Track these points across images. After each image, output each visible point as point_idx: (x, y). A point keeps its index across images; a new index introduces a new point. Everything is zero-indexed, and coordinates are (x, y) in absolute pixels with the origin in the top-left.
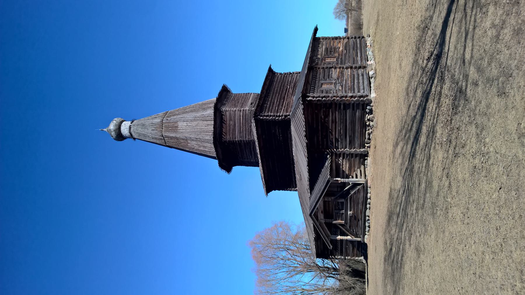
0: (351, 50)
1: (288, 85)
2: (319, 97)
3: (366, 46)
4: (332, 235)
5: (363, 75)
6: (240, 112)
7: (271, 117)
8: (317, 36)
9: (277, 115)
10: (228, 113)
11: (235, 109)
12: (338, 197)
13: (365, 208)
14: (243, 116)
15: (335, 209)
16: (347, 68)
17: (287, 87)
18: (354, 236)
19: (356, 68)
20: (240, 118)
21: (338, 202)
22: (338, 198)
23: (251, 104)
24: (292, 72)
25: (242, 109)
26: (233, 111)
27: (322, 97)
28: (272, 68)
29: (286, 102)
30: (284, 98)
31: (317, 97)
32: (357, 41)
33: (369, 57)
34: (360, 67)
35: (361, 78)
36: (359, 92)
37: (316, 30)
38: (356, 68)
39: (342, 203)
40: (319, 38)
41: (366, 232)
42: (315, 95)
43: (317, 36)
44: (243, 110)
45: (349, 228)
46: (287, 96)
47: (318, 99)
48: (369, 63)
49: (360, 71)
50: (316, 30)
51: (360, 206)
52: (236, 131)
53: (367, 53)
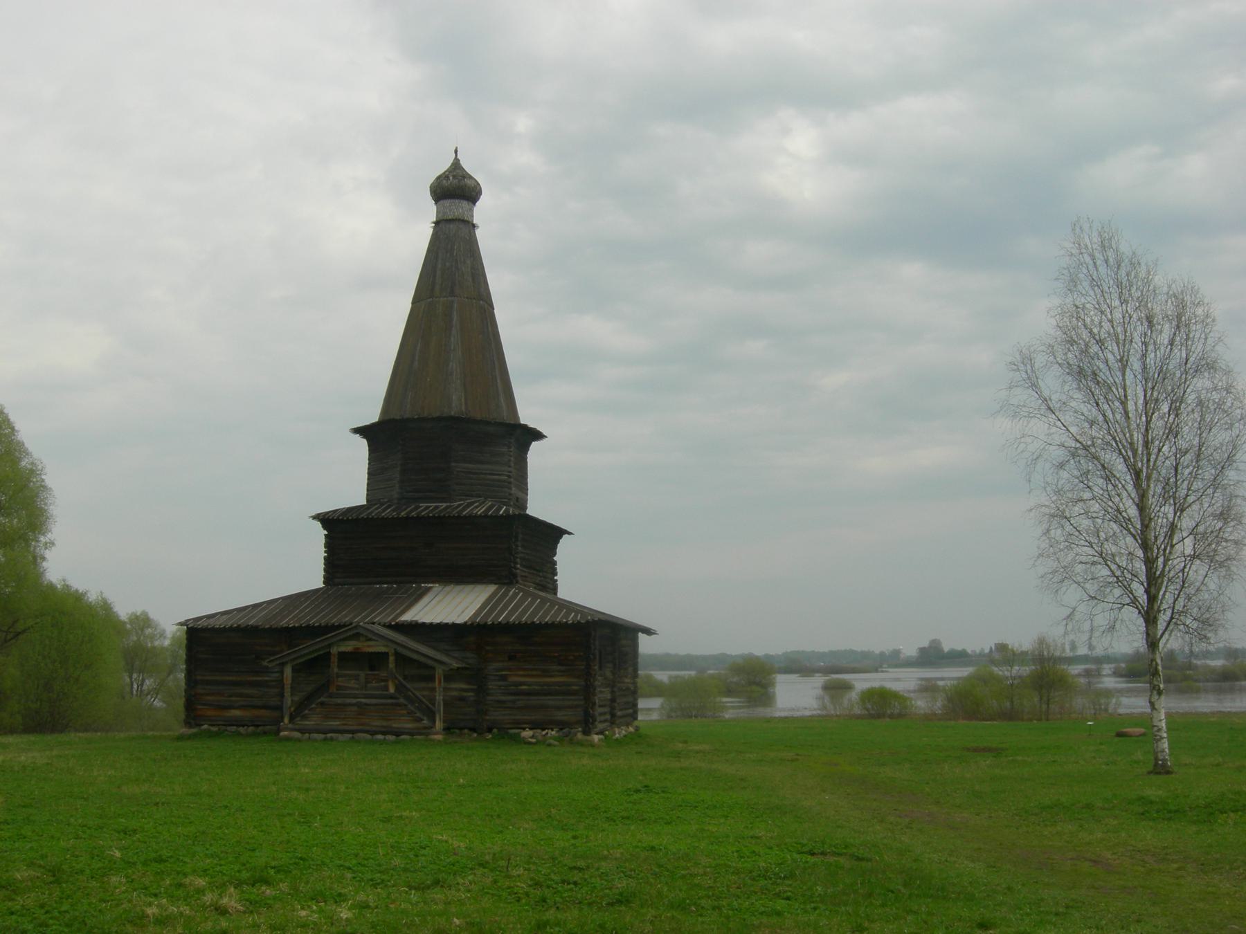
4: (292, 667)
7: (514, 547)
8: (640, 635)
9: (517, 558)
10: (505, 449)
11: (512, 464)
12: (399, 681)
14: (499, 481)
16: (613, 692)
17: (540, 571)
18: (294, 711)
19: (613, 708)
21: (386, 681)
22: (397, 681)
23: (517, 499)
24: (555, 578)
25: (512, 480)
28: (565, 537)
29: (525, 572)
34: (613, 715)
36: (601, 714)
37: (648, 632)
39: (386, 688)
43: (640, 635)
44: (510, 483)
45: (319, 700)
49: (608, 717)
50: (648, 632)
51: (378, 723)
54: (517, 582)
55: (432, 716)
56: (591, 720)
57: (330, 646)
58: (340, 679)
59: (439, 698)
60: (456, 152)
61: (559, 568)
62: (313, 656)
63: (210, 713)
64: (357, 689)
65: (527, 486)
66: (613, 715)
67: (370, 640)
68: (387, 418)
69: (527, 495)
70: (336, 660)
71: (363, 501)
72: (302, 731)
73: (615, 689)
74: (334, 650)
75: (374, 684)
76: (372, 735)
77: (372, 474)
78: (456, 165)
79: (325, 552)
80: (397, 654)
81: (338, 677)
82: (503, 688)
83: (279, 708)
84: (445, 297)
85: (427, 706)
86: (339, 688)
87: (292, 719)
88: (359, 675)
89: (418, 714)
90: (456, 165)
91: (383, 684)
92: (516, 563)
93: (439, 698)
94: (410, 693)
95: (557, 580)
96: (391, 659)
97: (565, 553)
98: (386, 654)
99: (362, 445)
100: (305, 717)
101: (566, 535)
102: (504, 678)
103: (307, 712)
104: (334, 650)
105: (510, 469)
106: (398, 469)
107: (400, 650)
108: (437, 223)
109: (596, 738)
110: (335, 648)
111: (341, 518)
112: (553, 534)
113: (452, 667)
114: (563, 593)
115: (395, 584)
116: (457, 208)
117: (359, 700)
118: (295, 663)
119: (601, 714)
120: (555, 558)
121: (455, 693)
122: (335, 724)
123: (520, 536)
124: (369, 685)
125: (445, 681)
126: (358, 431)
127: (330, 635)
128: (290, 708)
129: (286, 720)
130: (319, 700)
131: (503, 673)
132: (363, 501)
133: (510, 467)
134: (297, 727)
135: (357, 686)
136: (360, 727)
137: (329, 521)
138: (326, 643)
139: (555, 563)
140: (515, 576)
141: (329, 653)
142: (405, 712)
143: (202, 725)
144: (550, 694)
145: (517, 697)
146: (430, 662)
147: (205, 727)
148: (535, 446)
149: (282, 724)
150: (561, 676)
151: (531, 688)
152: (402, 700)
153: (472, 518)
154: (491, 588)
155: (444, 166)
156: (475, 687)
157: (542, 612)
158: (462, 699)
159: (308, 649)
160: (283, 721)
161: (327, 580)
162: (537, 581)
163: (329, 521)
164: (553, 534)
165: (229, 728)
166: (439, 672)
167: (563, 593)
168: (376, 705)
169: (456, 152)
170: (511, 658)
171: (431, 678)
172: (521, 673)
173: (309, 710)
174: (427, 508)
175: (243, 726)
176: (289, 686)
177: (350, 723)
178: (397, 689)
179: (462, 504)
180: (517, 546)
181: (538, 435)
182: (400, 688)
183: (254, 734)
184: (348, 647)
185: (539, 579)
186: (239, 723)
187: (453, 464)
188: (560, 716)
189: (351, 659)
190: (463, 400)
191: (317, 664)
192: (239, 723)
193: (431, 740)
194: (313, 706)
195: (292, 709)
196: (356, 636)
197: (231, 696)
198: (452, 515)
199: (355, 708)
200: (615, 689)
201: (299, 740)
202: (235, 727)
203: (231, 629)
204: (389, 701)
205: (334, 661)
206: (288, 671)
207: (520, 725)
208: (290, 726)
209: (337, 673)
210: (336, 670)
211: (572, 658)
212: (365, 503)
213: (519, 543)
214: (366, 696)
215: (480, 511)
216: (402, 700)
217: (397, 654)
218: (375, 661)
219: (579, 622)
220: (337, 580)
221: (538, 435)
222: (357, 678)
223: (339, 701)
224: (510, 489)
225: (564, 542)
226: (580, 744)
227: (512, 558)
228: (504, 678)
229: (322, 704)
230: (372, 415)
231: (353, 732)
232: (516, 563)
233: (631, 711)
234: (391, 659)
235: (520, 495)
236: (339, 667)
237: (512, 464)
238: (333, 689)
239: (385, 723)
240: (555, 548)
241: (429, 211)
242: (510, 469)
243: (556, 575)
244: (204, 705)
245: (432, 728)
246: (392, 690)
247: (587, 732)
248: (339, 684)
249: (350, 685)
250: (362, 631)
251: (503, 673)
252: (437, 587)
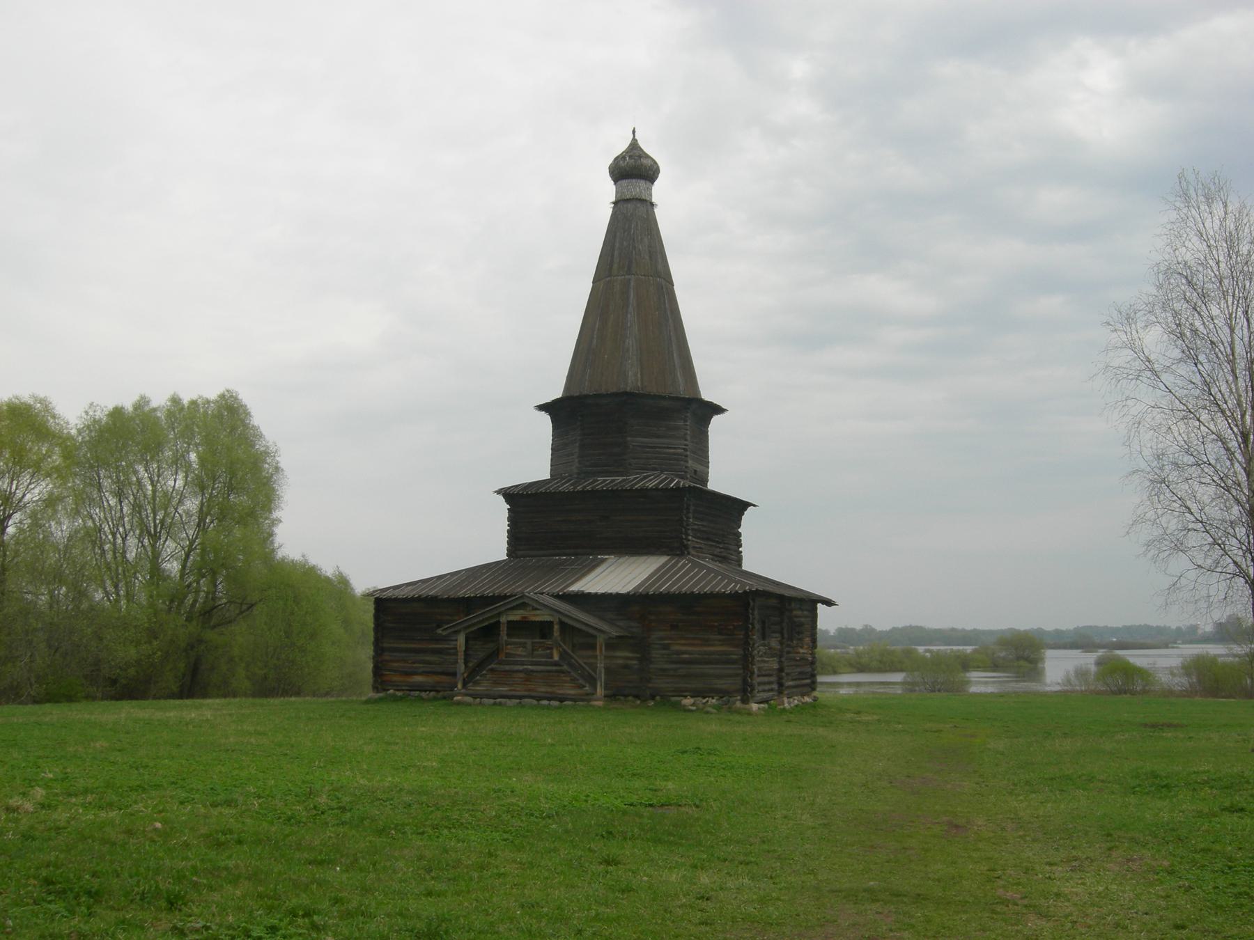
0: (799, 670)
1: (724, 543)
2: (754, 619)
3: (803, 695)
4: (466, 634)
5: (772, 690)
6: (684, 449)
7: (685, 519)
8: (819, 605)
9: (689, 529)
10: (681, 423)
12: (563, 649)
13: (539, 697)
14: (674, 454)
15: (533, 643)
16: (780, 662)
17: (720, 543)
19: (780, 678)
20: (671, 448)
21: (551, 649)
23: (695, 471)
24: (740, 549)
25: (688, 453)
26: (686, 434)
27: (752, 624)
28: (751, 508)
29: (701, 543)
30: (708, 539)
31: (753, 614)
32: (806, 679)
33: (791, 700)
34: (781, 685)
35: (767, 687)
36: (760, 684)
37: (829, 603)
38: (780, 678)
39: (551, 656)
40: (815, 609)
41: (481, 698)
42: (756, 612)
43: (819, 605)
44: (686, 456)
45: (490, 667)
46: (711, 546)
47: (751, 616)
48: (786, 700)
49: (775, 686)
50: (829, 603)
51: (543, 689)
52: (646, 438)
53: (796, 698)
54: (689, 554)
55: (592, 681)
56: (749, 689)
57: (499, 614)
58: (509, 647)
59: (601, 666)
60: (634, 132)
62: (486, 624)
63: (397, 678)
64: (524, 656)
65: (708, 459)
66: (781, 685)
67: (537, 609)
68: (568, 395)
69: (708, 467)
70: (506, 629)
71: (546, 475)
72: (474, 696)
73: (783, 659)
74: (503, 619)
75: (540, 652)
76: (538, 700)
78: (634, 145)
79: (508, 525)
80: (562, 623)
81: (507, 645)
82: (665, 656)
83: (454, 674)
84: (622, 275)
85: (589, 673)
86: (508, 655)
87: (464, 685)
88: (525, 643)
89: (581, 681)
90: (634, 145)
91: (548, 651)
92: (688, 535)
93: (601, 666)
94: (573, 661)
95: (741, 552)
96: (556, 627)
97: (749, 526)
98: (551, 623)
99: (545, 420)
100: (476, 683)
101: (752, 507)
102: (666, 647)
103: (478, 677)
104: (503, 619)
105: (685, 442)
106: (577, 445)
107: (564, 619)
108: (615, 203)
109: (755, 706)
110: (505, 616)
111: (521, 492)
112: (737, 507)
113: (611, 636)
114: (746, 566)
115: (573, 555)
116: (635, 187)
117: (525, 667)
118: (468, 631)
119: (760, 684)
120: (740, 530)
121: (620, 661)
122: (503, 689)
123: (692, 508)
124: (536, 652)
125: (606, 649)
126: (542, 408)
127: (499, 604)
128: (463, 674)
129: (460, 686)
130: (490, 667)
131: (666, 642)
132: (546, 475)
133: (686, 440)
134: (471, 692)
135: (524, 654)
136: (526, 693)
137: (514, 497)
138: (496, 612)
139: (739, 535)
140: (686, 547)
141: (498, 622)
142: (569, 679)
143: (389, 690)
144: (707, 663)
145: (678, 666)
146: (591, 631)
147: (391, 691)
148: (716, 420)
149: (456, 689)
150: (721, 645)
151: (691, 656)
152: (565, 667)
153: (644, 492)
154: (664, 559)
155: (621, 146)
156: (638, 655)
157: (704, 582)
158: (626, 667)
159: (479, 618)
160: (456, 687)
161: (511, 553)
162: (715, 553)
163: (514, 497)
164: (737, 507)
165: (412, 693)
166: (601, 640)
167: (746, 566)
168: (541, 671)
169: (634, 132)
170: (674, 627)
171: (592, 647)
172: (683, 642)
173: (481, 676)
174: (603, 482)
175: (426, 691)
176: (463, 653)
177: (518, 689)
178: (561, 656)
179: (638, 477)
180: (688, 518)
181: (718, 410)
182: (563, 655)
183: (435, 699)
184: (516, 616)
185: (718, 550)
186: (421, 688)
187: (629, 439)
188: (721, 684)
189: (517, 628)
190: (639, 375)
191: (490, 631)
192: (421, 688)
193: (591, 706)
194: (484, 672)
195: (465, 675)
196: (523, 606)
197: (414, 663)
198: (624, 488)
199: (522, 675)
200: (783, 659)
201: (469, 704)
202: (418, 692)
203: (413, 599)
204: (554, 668)
205: (504, 630)
206: (461, 639)
207: (682, 693)
208: (463, 691)
209: (506, 641)
210: (505, 638)
211: (731, 627)
212: (549, 478)
213: (691, 515)
214: (533, 664)
215: (651, 485)
216: (565, 667)
217: (562, 623)
218: (544, 629)
219: (737, 592)
220: (520, 553)
221: (718, 410)
222: (523, 645)
223: (507, 668)
224: (687, 462)
226: (738, 712)
227: (683, 530)
228: (666, 647)
229: (492, 670)
230: (555, 390)
231: (520, 697)
232: (688, 535)
233: (808, 681)
234: (556, 627)
235: (699, 467)
236: (509, 635)
237: (688, 438)
238: (502, 657)
239: (549, 690)
240: (740, 520)
241: (608, 191)
242: (685, 442)
243: (741, 546)
244: (390, 670)
245: (593, 694)
246: (556, 657)
247: (745, 701)
248: (507, 651)
249: (518, 653)
250: (526, 600)
251: (666, 642)
252: (611, 558)
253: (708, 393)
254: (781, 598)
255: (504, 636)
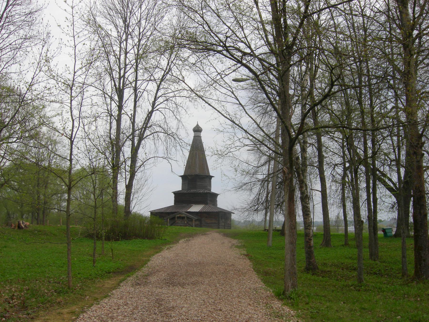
59: (194, 224)
61: (218, 201)
71: (181, 189)
77: (182, 184)
78: (198, 125)
90: (198, 125)
93: (194, 224)
97: (219, 199)
104: (176, 216)
114: (218, 206)
116: (198, 134)
132: (181, 189)
137: (175, 193)
153: (200, 193)
154: (204, 205)
155: (195, 125)
159: (171, 216)
161: (175, 203)
163: (175, 193)
166: (194, 220)
167: (218, 206)
174: (192, 191)
181: (213, 177)
182: (187, 222)
184: (178, 216)
189: (179, 218)
191: (173, 218)
196: (180, 214)
203: (158, 213)
205: (176, 218)
206: (168, 220)
215: (201, 192)
218: (183, 218)
225: (218, 197)
241: (192, 135)
252: (194, 205)
253: (211, 174)
254: (225, 212)
255: (176, 219)
